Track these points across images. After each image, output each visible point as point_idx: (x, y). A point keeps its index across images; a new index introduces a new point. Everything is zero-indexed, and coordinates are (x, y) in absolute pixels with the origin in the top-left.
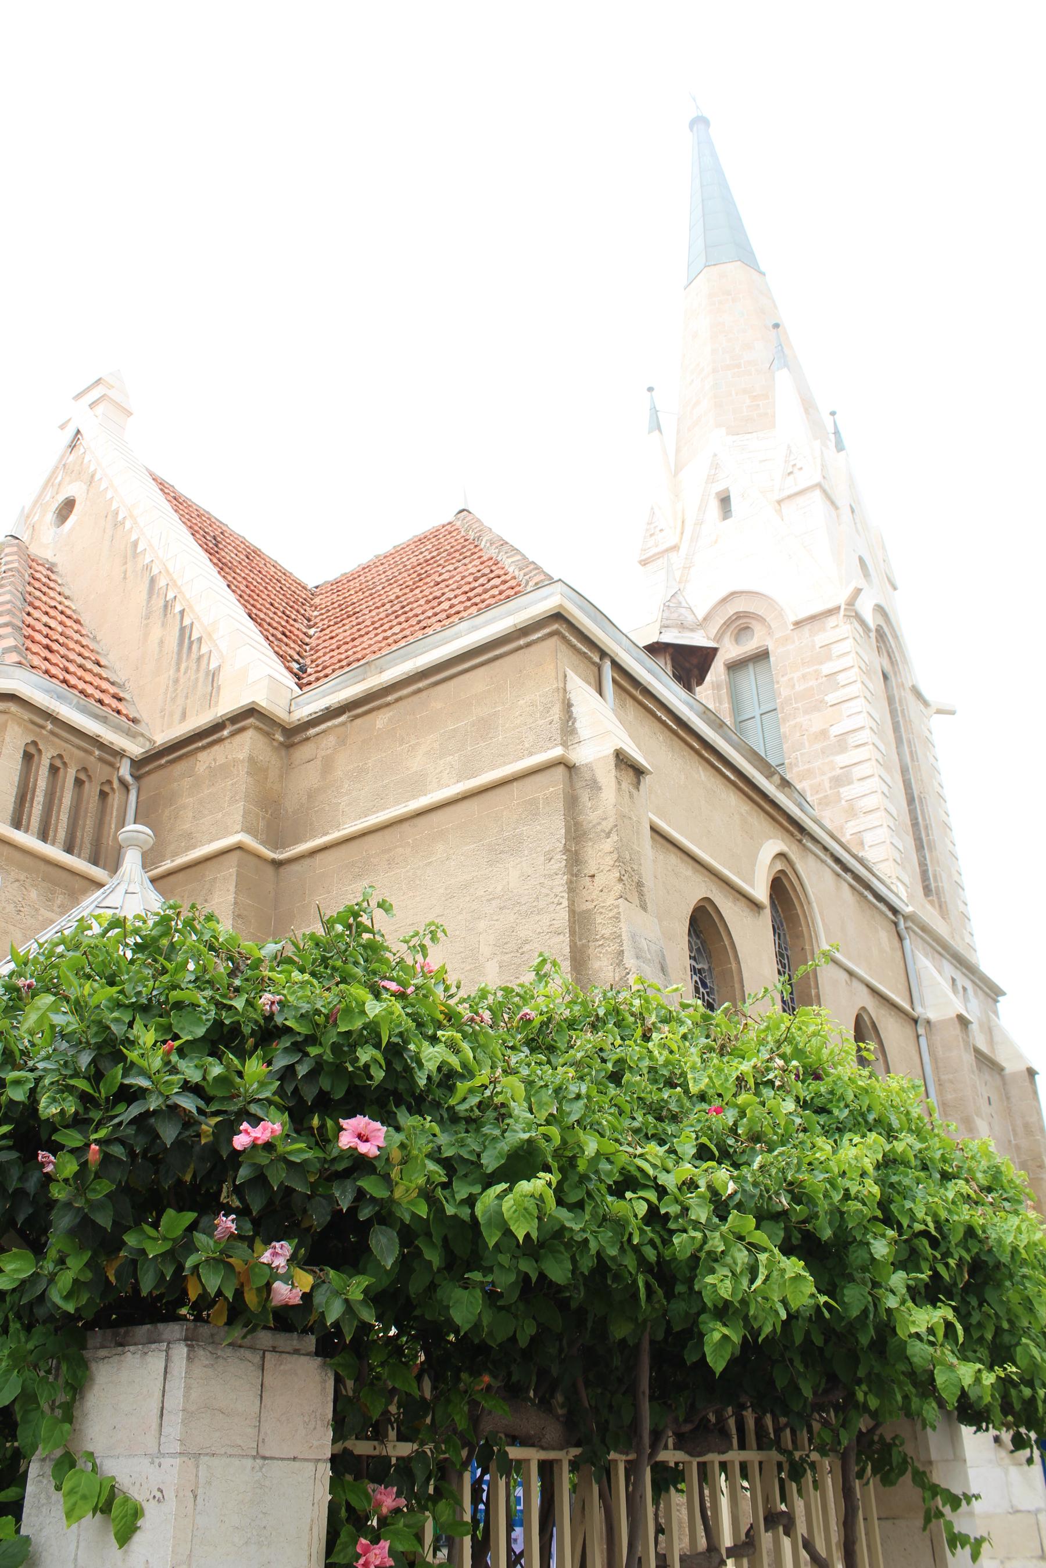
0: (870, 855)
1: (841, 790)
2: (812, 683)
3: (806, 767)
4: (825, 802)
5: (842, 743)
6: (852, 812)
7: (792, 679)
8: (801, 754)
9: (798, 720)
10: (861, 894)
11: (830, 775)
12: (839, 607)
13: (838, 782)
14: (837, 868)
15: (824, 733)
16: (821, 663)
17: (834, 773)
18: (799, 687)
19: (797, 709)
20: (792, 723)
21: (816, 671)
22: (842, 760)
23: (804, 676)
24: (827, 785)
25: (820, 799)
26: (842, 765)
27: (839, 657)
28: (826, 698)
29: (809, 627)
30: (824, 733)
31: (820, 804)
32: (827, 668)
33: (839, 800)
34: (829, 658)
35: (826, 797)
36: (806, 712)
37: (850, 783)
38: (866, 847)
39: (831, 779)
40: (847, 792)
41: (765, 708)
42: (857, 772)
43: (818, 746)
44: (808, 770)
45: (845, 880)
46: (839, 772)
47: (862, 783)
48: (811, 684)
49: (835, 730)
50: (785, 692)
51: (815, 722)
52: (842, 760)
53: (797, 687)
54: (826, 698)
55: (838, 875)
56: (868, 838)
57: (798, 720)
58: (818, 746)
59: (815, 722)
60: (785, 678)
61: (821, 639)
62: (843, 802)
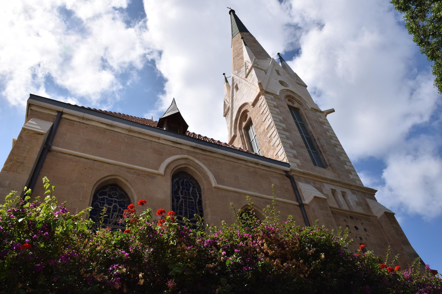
13: (270, 142)
15: (264, 130)
40: (272, 144)
58: (264, 135)
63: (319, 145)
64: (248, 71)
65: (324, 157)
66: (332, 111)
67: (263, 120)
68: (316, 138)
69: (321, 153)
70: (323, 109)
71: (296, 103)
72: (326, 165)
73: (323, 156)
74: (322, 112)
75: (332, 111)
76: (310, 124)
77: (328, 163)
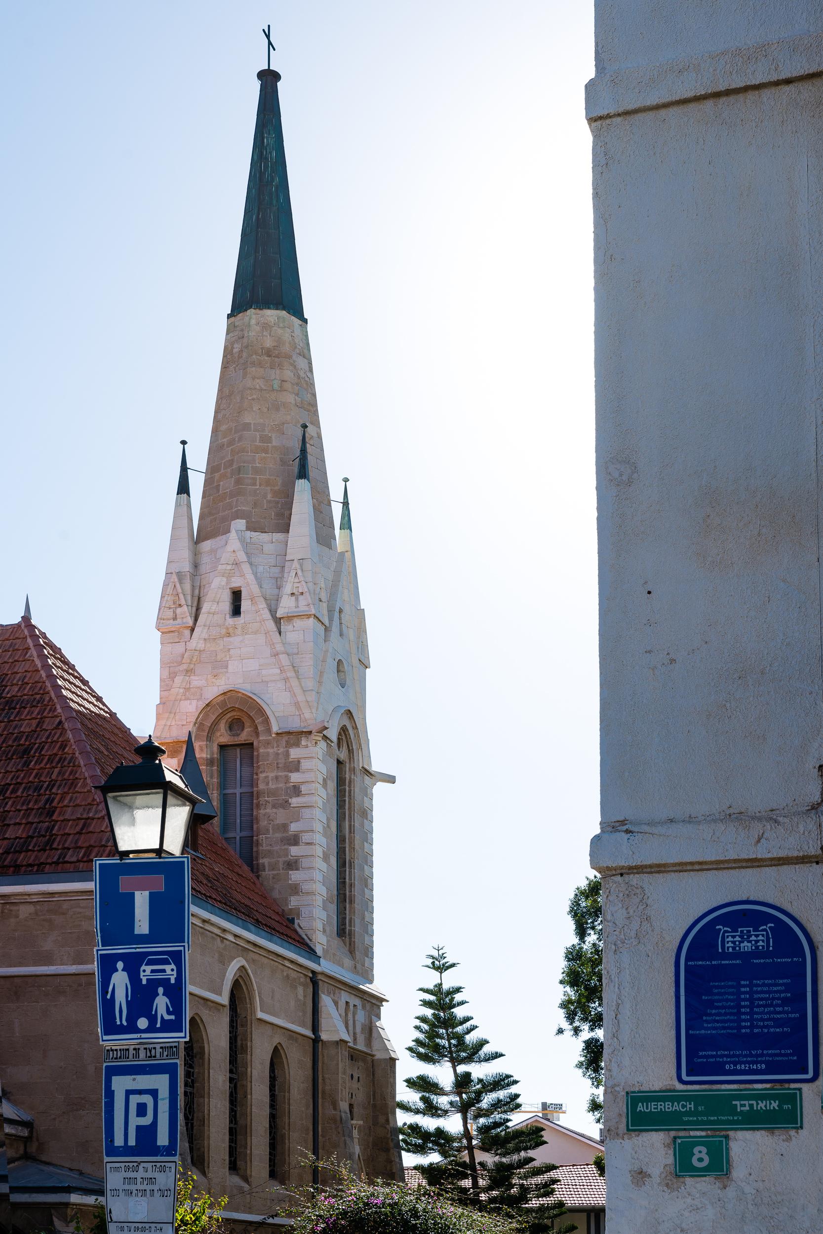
8: (266, 838)
9: (268, 811)
17: (286, 859)
18: (272, 786)
19: (267, 801)
23: (277, 778)
24: (281, 866)
31: (273, 878)
36: (274, 806)
39: (284, 862)
43: (278, 835)
44: (269, 851)
50: (262, 786)
51: (280, 816)
53: (270, 784)
57: (268, 811)
58: (278, 835)
59: (280, 816)
60: (264, 775)
65: (347, 912)
66: (391, 779)
70: (376, 766)
75: (391, 779)
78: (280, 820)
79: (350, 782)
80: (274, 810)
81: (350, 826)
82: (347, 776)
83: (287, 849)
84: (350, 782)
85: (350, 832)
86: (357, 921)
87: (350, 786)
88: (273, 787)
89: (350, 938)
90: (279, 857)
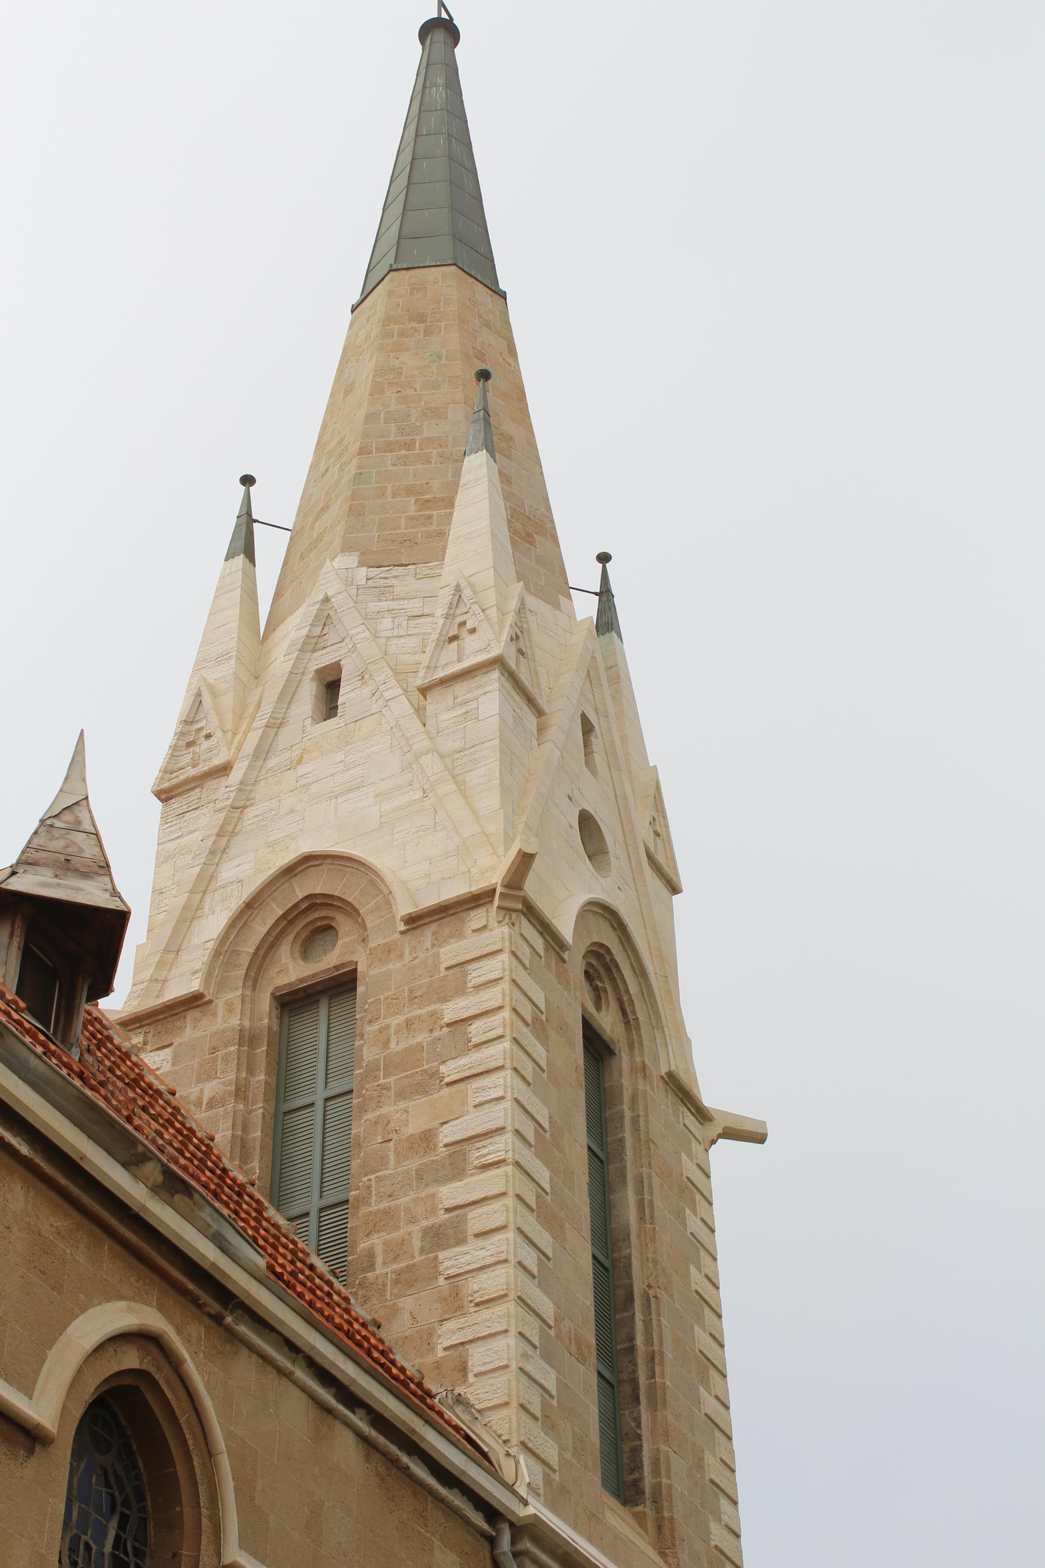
0: (479, 1392)
1: (442, 1255)
2: (422, 1037)
3: (382, 1206)
4: (407, 1280)
5: (456, 1161)
6: (455, 1303)
7: (387, 1027)
8: (379, 1179)
10: (394, 1462)
11: (424, 1223)
12: (494, 890)
13: (440, 1237)
14: (327, 1396)
15: (428, 1137)
16: (445, 999)
17: (432, 1221)
18: (396, 1046)
19: (385, 1088)
20: (371, 1116)
21: (432, 1014)
22: (451, 1193)
23: (409, 1024)
24: (417, 1243)
25: (399, 1273)
26: (449, 1203)
27: (478, 987)
28: (443, 1069)
29: (433, 927)
30: (428, 1137)
31: (396, 1282)
32: (453, 1009)
33: (436, 1273)
34: (460, 990)
35: (410, 1268)
36: (401, 1095)
37: (461, 1241)
38: (471, 1378)
40: (451, 1260)
41: (335, 1088)
42: (478, 1219)
43: (413, 1164)
45: (348, 1424)
46: (443, 1217)
47: (481, 1242)
48: (419, 1039)
49: (449, 1134)
51: (413, 1116)
52: (451, 1193)
53: (393, 1045)
54: (443, 1069)
55: (329, 1411)
56: (478, 1358)
57: (385, 1110)
58: (413, 1164)
59: (413, 1116)
61: (451, 952)
62: (441, 1281)
63: (639, 1340)
64: (450, 663)
65: (645, 1432)
66: (753, 1135)
67: (451, 1069)
68: (638, 1288)
69: (637, 1399)
71: (613, 1005)
72: (636, 1486)
73: (638, 1421)
74: (702, 1114)
76: (640, 1182)
77: (648, 1481)
78: (412, 1129)
79: (634, 1099)
80: (402, 1105)
81: (641, 1204)
82: (625, 1081)
83: (433, 1196)
84: (634, 1099)
85: (642, 1218)
86: (678, 1465)
87: (633, 1107)
88: (402, 1046)
89: (659, 1510)
90: (413, 1221)
